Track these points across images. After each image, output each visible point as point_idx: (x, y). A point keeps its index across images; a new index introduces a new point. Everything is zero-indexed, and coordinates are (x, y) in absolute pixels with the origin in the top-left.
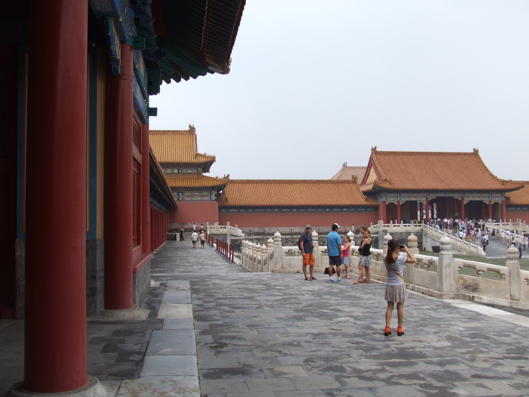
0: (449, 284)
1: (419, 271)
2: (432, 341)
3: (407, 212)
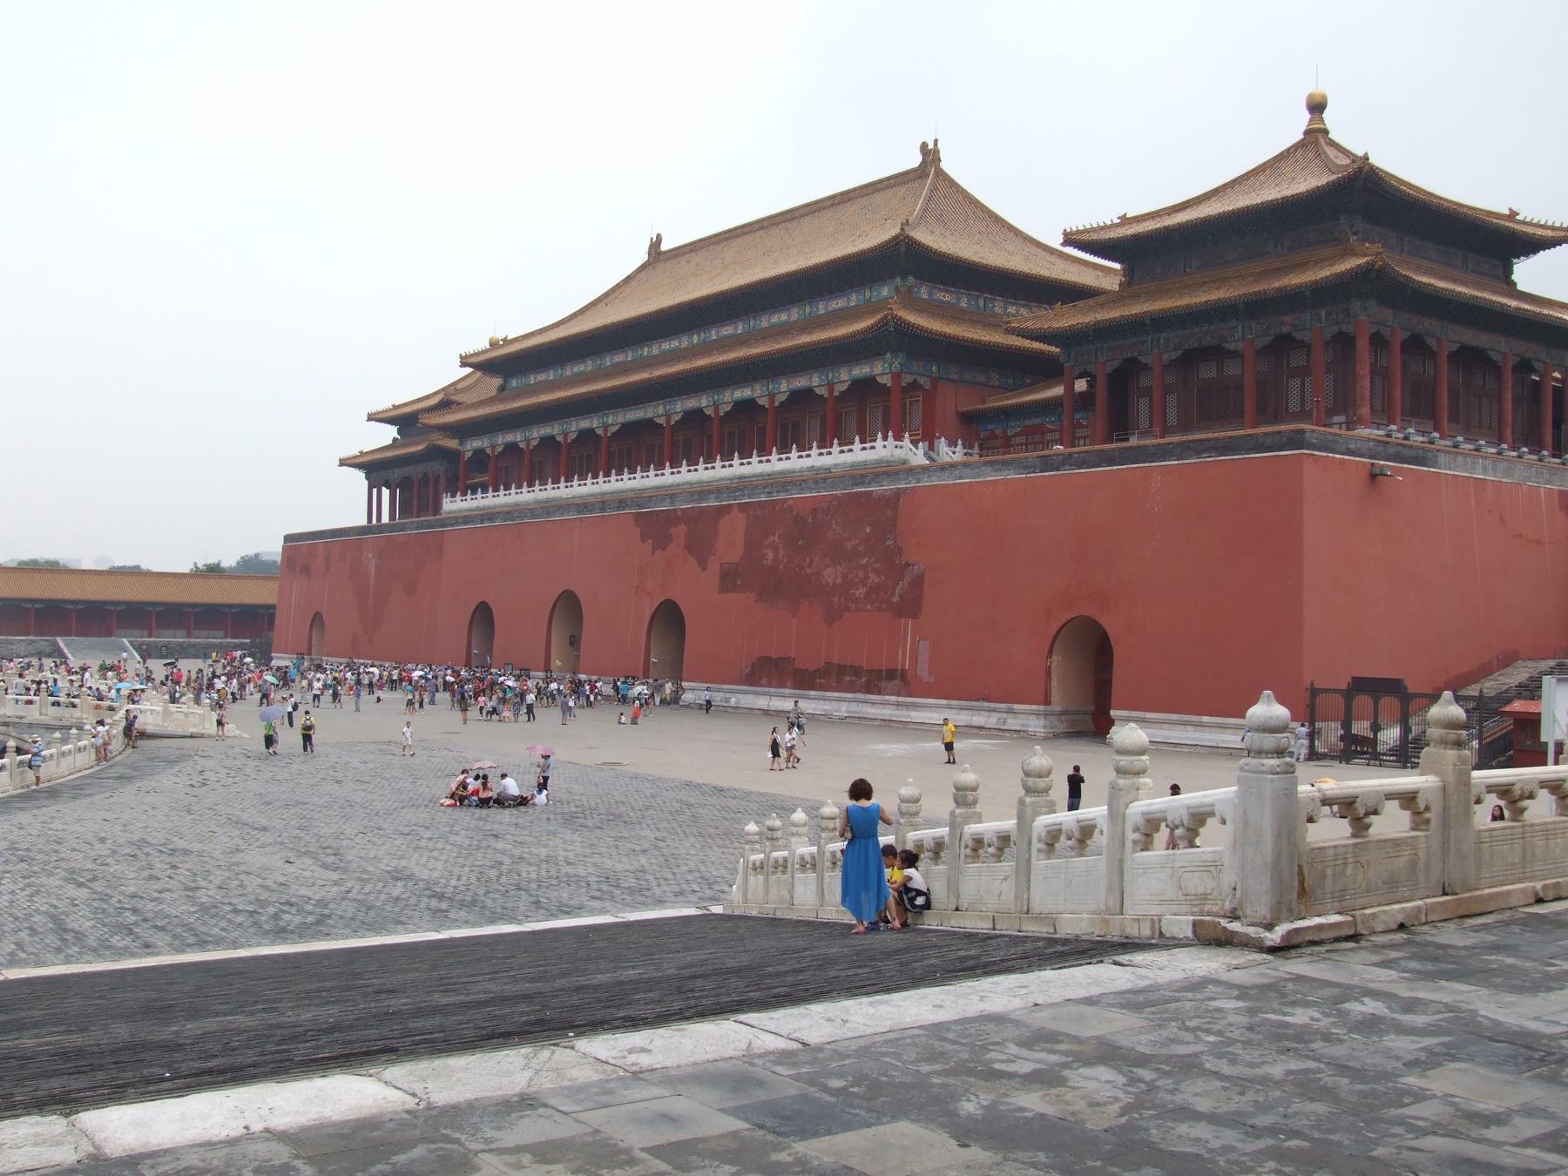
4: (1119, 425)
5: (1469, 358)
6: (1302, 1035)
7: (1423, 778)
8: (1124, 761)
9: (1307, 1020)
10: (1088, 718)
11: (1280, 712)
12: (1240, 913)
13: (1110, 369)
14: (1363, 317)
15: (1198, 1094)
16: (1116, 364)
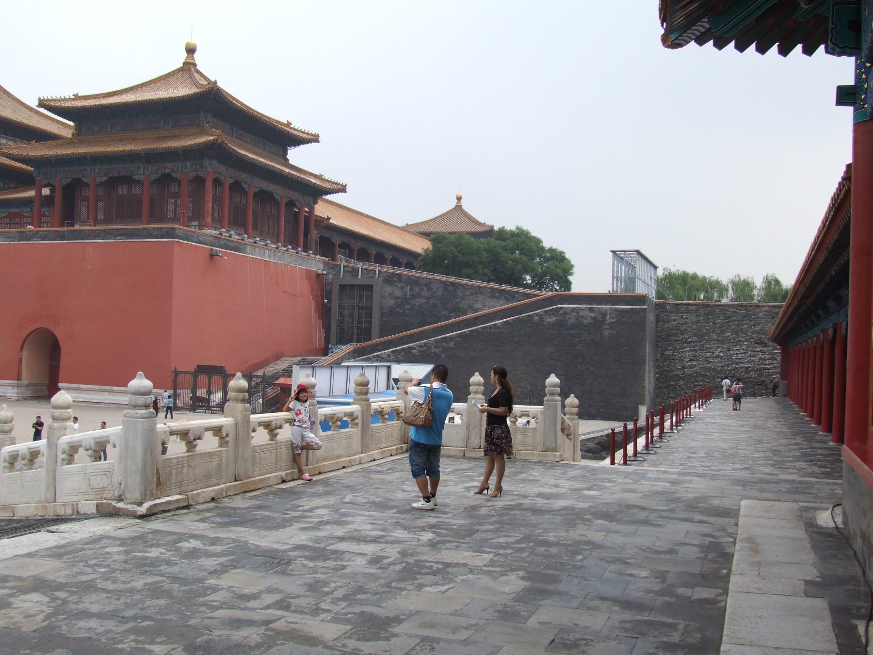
4: (69, 216)
6: (154, 563)
7: (225, 419)
8: (58, 413)
9: (158, 554)
10: (45, 388)
11: (147, 383)
12: (123, 497)
13: (64, 183)
14: (210, 169)
15: (93, 603)
16: (68, 181)
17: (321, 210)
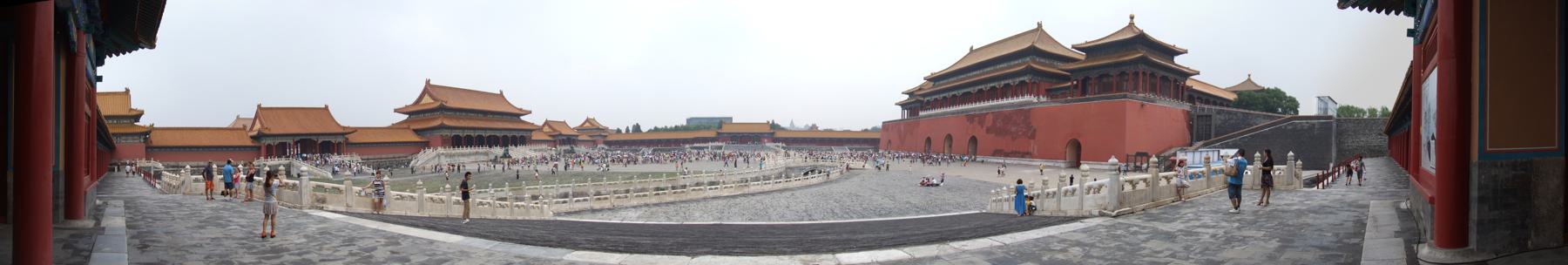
0: (307, 199)
1: (287, 191)
2: (295, 239)
3: (280, 150)
4: (1084, 92)
5: (1164, 78)
17: (1188, 83)
